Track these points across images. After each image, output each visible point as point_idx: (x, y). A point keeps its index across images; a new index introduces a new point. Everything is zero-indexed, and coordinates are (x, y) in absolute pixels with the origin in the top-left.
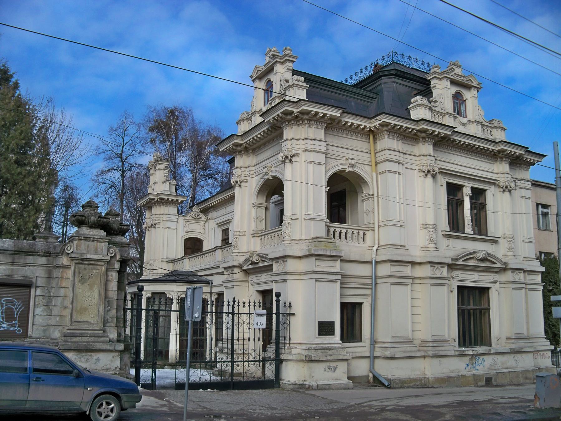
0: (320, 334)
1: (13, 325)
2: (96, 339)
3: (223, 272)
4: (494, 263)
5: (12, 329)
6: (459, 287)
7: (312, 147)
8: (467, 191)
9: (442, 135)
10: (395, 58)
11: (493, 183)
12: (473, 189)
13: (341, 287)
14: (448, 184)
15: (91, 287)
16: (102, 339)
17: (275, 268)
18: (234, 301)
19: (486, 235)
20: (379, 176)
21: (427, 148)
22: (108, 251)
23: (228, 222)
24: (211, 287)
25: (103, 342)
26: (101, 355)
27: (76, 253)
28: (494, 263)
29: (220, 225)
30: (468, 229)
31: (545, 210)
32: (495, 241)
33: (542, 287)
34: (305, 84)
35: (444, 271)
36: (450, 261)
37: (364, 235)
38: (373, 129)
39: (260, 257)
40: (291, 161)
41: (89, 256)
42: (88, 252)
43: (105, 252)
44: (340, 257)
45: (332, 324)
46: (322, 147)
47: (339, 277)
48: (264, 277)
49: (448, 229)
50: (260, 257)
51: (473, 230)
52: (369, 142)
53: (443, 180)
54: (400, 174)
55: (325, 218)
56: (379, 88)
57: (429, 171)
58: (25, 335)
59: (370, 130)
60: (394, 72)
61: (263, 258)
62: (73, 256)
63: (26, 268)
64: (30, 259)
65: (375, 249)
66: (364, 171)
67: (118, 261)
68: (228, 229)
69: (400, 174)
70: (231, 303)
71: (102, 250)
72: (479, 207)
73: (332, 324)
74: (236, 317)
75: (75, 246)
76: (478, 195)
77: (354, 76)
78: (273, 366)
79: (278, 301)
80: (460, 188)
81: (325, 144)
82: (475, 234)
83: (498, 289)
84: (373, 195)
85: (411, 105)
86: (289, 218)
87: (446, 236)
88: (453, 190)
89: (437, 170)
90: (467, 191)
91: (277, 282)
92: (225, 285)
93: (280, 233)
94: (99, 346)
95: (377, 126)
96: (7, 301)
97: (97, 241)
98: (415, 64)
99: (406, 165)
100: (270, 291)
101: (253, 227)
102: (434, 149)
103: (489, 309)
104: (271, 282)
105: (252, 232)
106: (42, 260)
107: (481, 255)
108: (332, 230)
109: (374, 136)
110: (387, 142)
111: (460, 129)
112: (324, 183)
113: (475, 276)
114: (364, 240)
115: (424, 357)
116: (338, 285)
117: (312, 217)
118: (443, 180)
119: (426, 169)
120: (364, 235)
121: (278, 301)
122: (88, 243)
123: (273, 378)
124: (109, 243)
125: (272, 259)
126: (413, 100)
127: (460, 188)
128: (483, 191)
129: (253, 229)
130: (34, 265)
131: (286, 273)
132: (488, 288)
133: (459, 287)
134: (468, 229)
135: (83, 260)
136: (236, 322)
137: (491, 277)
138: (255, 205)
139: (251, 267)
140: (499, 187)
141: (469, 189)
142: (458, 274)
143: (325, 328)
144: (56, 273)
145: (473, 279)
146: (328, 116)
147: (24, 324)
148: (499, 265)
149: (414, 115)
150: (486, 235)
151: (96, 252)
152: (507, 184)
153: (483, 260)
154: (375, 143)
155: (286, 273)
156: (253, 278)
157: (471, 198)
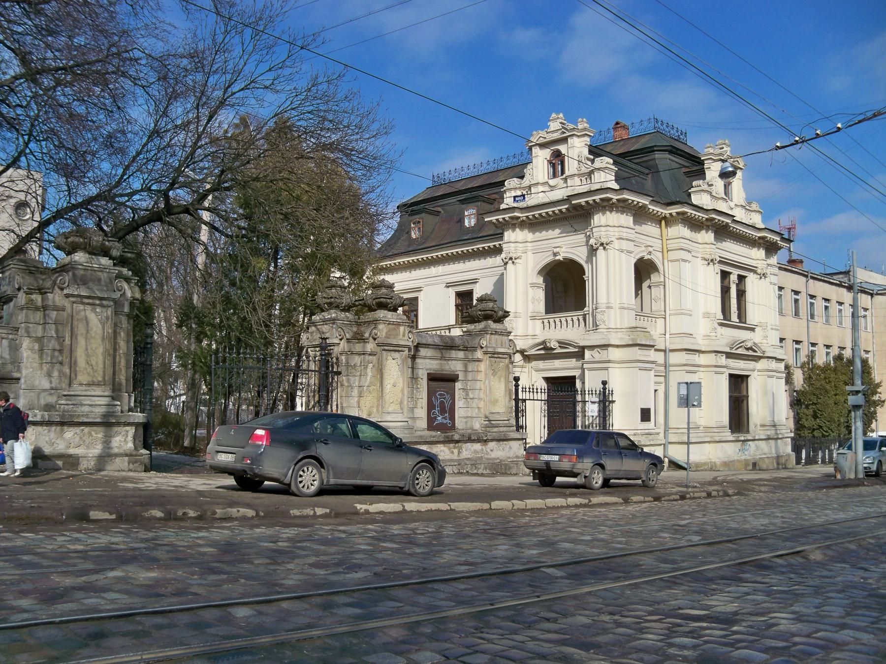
1: (445, 418)
4: (755, 351)
5: (445, 422)
7: (624, 235)
8: (734, 278)
11: (752, 270)
12: (739, 275)
15: (500, 378)
17: (587, 354)
19: (745, 323)
21: (708, 236)
23: (419, 290)
26: (512, 443)
28: (755, 351)
32: (753, 330)
33: (784, 375)
34: (613, 167)
35: (723, 360)
36: (728, 350)
38: (668, 215)
40: (604, 248)
44: (653, 346)
46: (631, 234)
47: (653, 366)
48: (557, 363)
50: (559, 342)
52: (661, 227)
53: (718, 268)
54: (689, 262)
56: (651, 163)
58: (453, 427)
60: (670, 148)
61: (562, 344)
63: (450, 362)
64: (454, 354)
66: (657, 258)
68: (416, 299)
69: (689, 262)
72: (741, 294)
79: (604, 389)
81: (633, 232)
85: (692, 190)
86: (604, 306)
87: (721, 325)
89: (718, 259)
90: (734, 278)
95: (674, 214)
96: (440, 395)
99: (693, 254)
101: (531, 308)
102: (715, 237)
105: (530, 314)
106: (461, 354)
107: (749, 345)
110: (680, 230)
115: (709, 442)
116: (652, 373)
117: (626, 306)
118: (718, 268)
121: (604, 389)
122: (496, 336)
125: (583, 348)
126: (694, 183)
128: (745, 277)
129: (530, 309)
130: (456, 359)
131: (609, 362)
132: (747, 376)
133: (731, 376)
134: (734, 317)
137: (750, 365)
138: (533, 285)
139: (542, 352)
140: (758, 274)
142: (732, 363)
143: (645, 415)
145: (739, 367)
147: (452, 418)
148: (759, 354)
149: (695, 199)
151: (502, 346)
153: (750, 349)
155: (609, 362)
156: (534, 364)
157: (737, 285)
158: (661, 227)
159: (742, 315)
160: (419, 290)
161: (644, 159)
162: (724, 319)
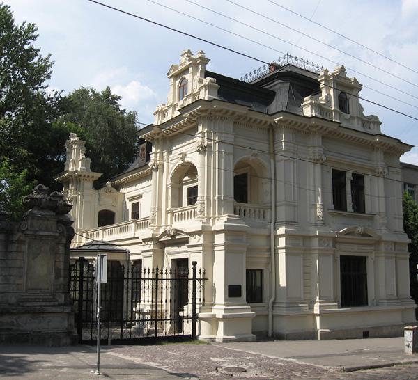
0: (229, 296)
2: (48, 304)
3: (141, 243)
6: (341, 256)
8: (349, 176)
9: (330, 129)
10: (290, 60)
12: (353, 174)
13: (247, 257)
14: (333, 170)
16: (52, 303)
18: (157, 269)
19: (364, 213)
20: (277, 163)
22: (58, 228)
23: (140, 197)
24: (129, 256)
25: (54, 306)
27: (31, 231)
29: (131, 199)
30: (350, 208)
31: (411, 189)
37: (264, 213)
39: (177, 231)
41: (41, 233)
42: (40, 230)
43: (54, 228)
45: (239, 287)
49: (333, 207)
51: (353, 208)
55: (233, 199)
56: (277, 86)
57: (318, 160)
59: (271, 125)
61: (178, 232)
62: (28, 232)
65: (273, 224)
66: (263, 159)
67: (64, 236)
70: (155, 271)
71: (52, 227)
73: (239, 287)
74: (159, 282)
75: (29, 224)
76: (358, 180)
77: (253, 73)
78: (191, 323)
79: (194, 269)
80: (343, 174)
82: (355, 212)
83: (373, 257)
84: (271, 179)
85: (304, 104)
88: (338, 176)
90: (349, 176)
91: (192, 252)
92: (143, 254)
93: (193, 210)
94: (50, 309)
97: (48, 220)
98: (307, 65)
100: (186, 260)
103: (366, 274)
104: (186, 252)
108: (238, 209)
109: (273, 130)
111: (345, 124)
112: (232, 169)
113: (356, 248)
114: (264, 217)
119: (317, 157)
120: (264, 213)
121: (194, 269)
123: (191, 333)
124: (59, 222)
125: (187, 234)
126: (306, 99)
127: (343, 174)
134: (350, 208)
135: (36, 236)
136: (159, 286)
141: (351, 174)
144: (14, 248)
146: (237, 113)
150: (364, 213)
151: (47, 230)
152: (381, 170)
154: (274, 136)
157: (352, 182)
158: (269, 134)
159: (359, 206)
160: (140, 197)
161: (273, 84)
162: (335, 209)
